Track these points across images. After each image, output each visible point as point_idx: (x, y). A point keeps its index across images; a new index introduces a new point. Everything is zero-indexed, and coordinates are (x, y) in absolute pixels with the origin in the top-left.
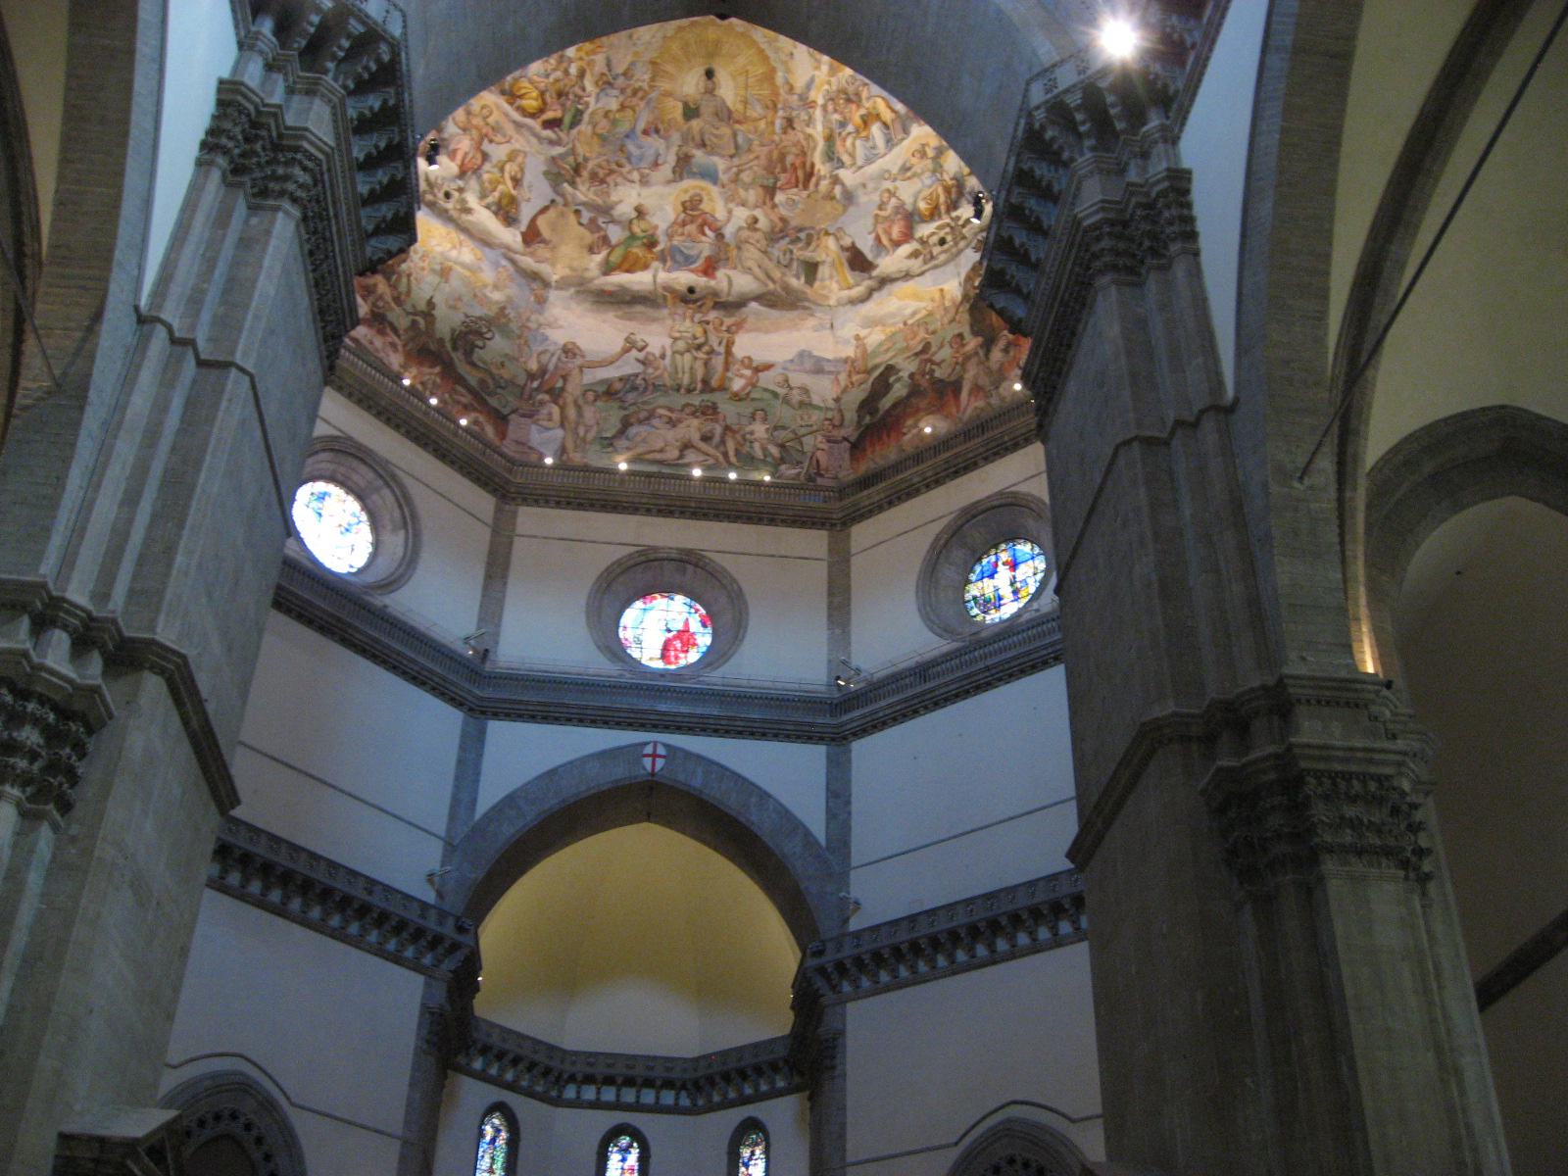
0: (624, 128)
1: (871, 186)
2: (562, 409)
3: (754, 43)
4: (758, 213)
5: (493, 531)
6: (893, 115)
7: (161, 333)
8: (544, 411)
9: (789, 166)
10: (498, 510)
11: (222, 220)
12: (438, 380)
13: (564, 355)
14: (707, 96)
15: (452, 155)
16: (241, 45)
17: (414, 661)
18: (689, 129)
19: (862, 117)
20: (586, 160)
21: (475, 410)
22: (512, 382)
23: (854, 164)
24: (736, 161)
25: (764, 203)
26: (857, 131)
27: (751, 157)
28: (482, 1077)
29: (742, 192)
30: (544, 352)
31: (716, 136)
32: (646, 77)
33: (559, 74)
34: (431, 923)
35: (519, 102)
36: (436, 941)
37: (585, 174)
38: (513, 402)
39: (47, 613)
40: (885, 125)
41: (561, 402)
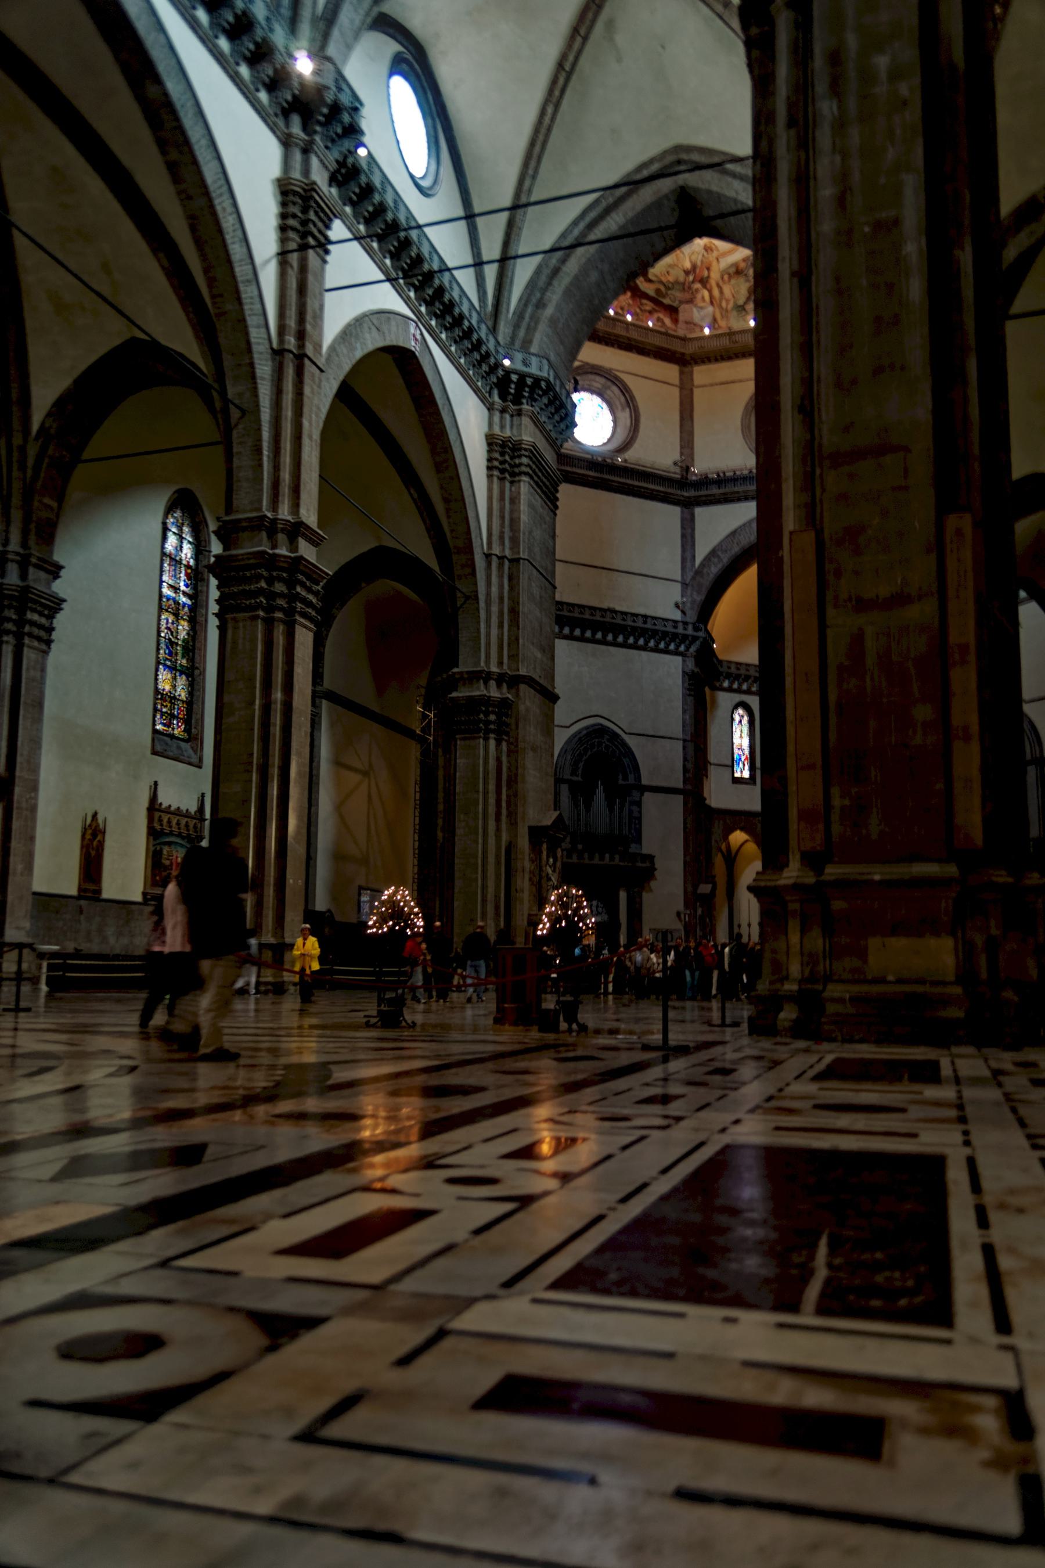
2: (710, 291)
5: (682, 388)
7: (494, 558)
8: (699, 296)
10: (681, 373)
11: (502, 498)
12: (631, 302)
13: (705, 254)
16: (489, 409)
17: (647, 488)
21: (656, 311)
22: (677, 282)
28: (730, 690)
30: (693, 253)
34: (680, 630)
36: (685, 637)
38: (678, 294)
39: (486, 677)
41: (708, 286)
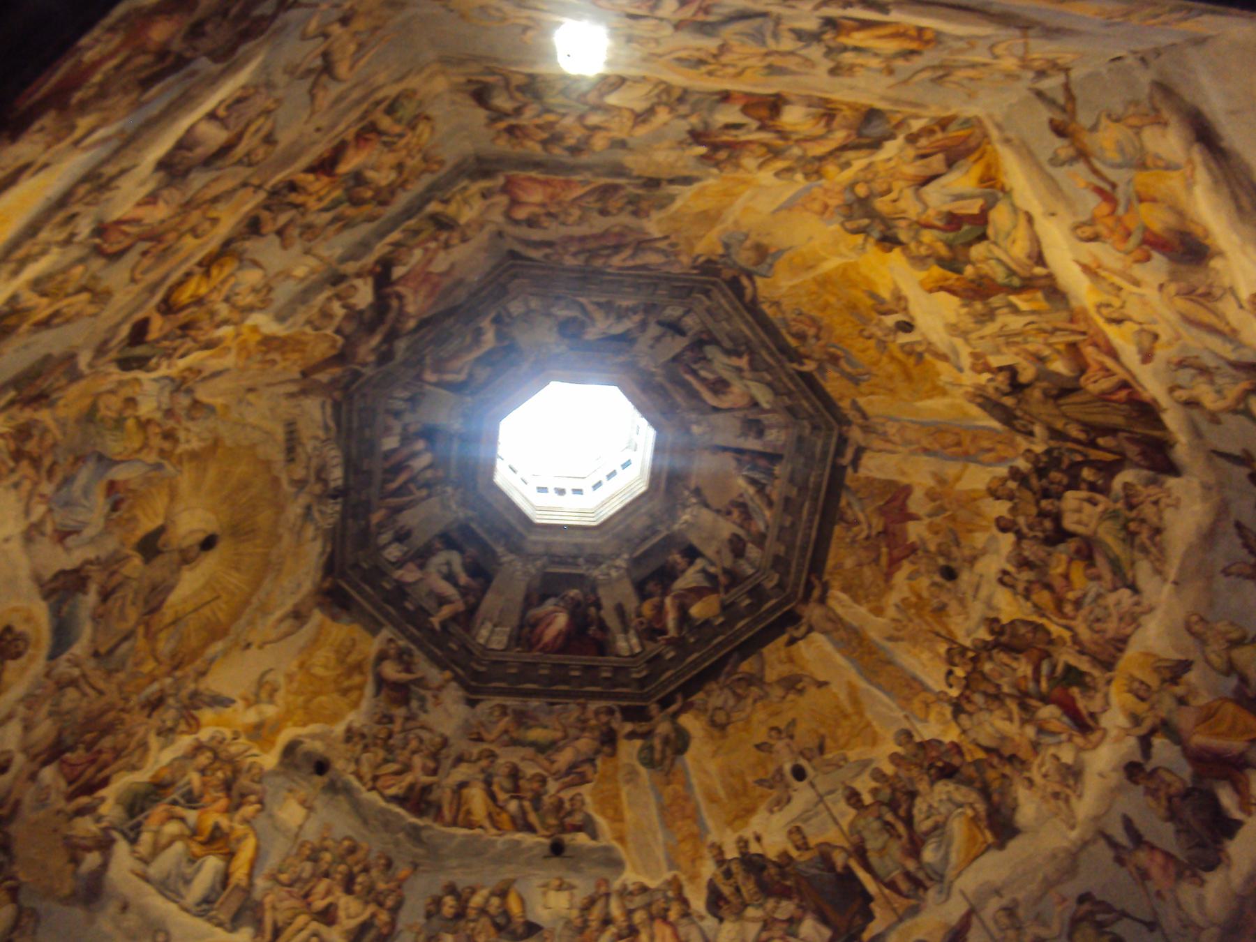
0: (113, 446)
1: (131, 920)
3: (256, 584)
4: (19, 759)
6: (244, 883)
9: (96, 748)
14: (176, 557)
15: (151, 199)
18: (128, 557)
19: (217, 827)
20: (52, 405)
23: (146, 861)
24: (92, 663)
25: (35, 757)
26: (195, 832)
27: (101, 685)
29: (46, 708)
31: (123, 605)
32: (195, 444)
33: (223, 310)
35: (199, 270)
37: (26, 414)
40: (225, 878)
